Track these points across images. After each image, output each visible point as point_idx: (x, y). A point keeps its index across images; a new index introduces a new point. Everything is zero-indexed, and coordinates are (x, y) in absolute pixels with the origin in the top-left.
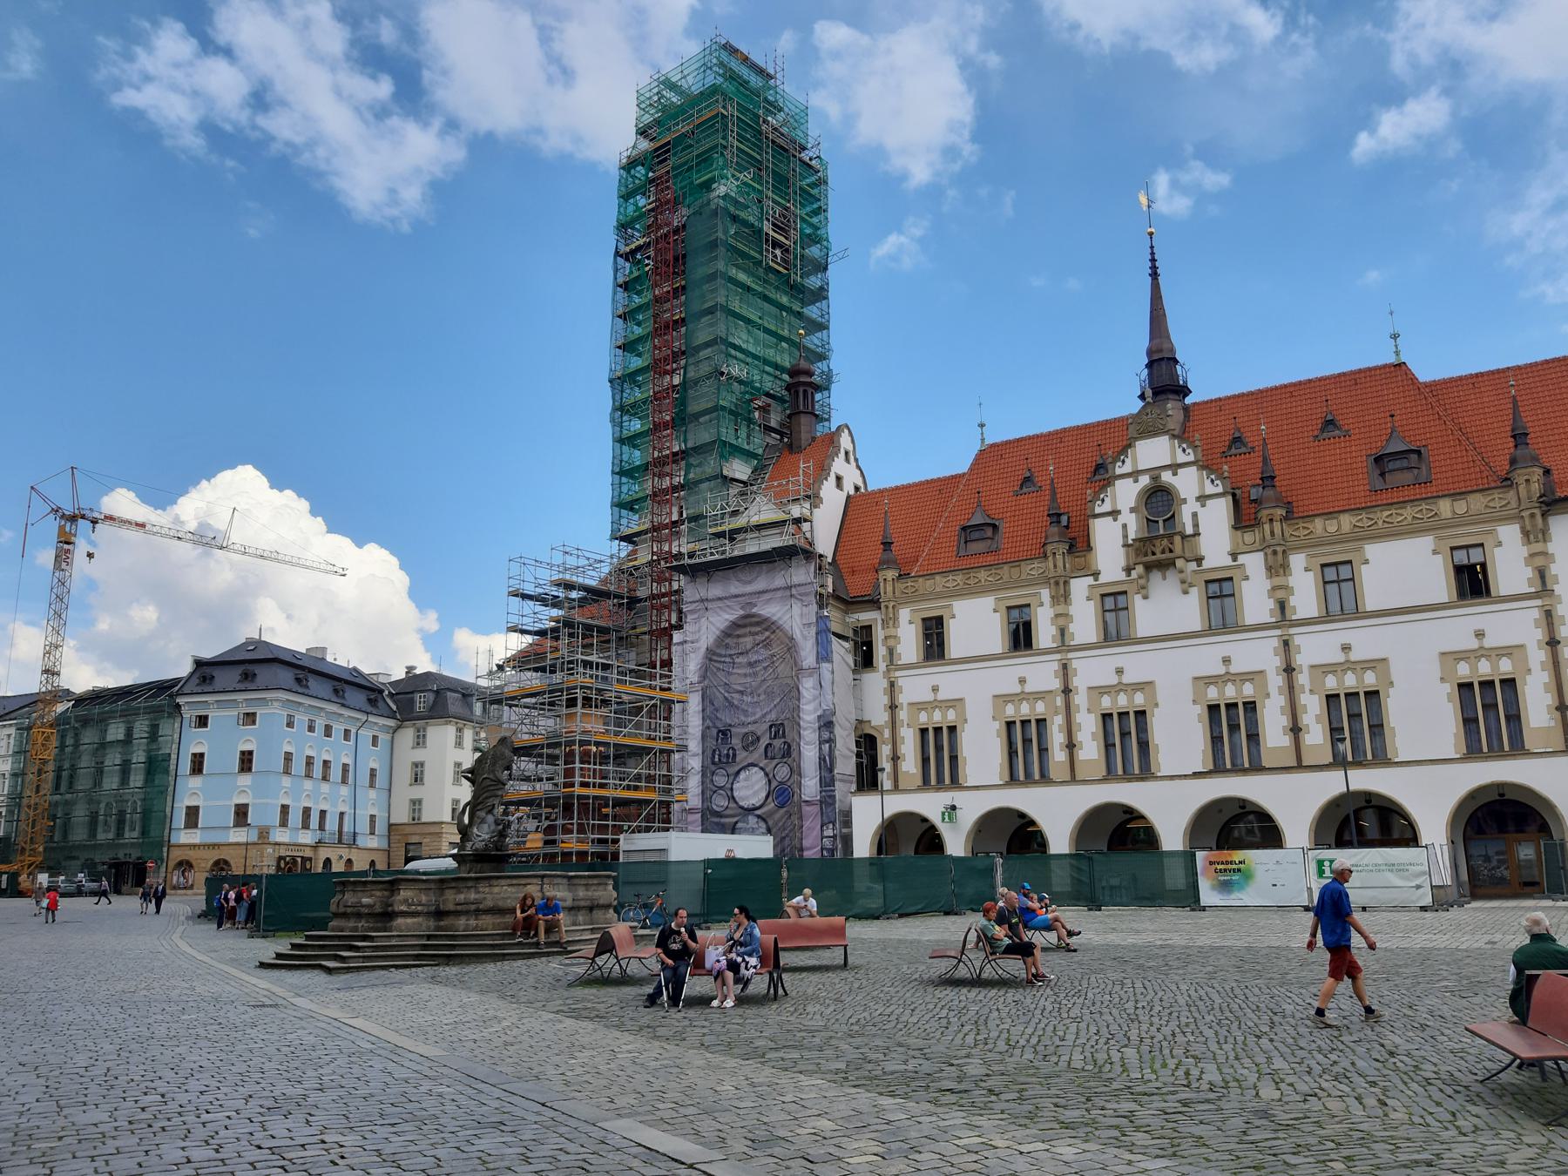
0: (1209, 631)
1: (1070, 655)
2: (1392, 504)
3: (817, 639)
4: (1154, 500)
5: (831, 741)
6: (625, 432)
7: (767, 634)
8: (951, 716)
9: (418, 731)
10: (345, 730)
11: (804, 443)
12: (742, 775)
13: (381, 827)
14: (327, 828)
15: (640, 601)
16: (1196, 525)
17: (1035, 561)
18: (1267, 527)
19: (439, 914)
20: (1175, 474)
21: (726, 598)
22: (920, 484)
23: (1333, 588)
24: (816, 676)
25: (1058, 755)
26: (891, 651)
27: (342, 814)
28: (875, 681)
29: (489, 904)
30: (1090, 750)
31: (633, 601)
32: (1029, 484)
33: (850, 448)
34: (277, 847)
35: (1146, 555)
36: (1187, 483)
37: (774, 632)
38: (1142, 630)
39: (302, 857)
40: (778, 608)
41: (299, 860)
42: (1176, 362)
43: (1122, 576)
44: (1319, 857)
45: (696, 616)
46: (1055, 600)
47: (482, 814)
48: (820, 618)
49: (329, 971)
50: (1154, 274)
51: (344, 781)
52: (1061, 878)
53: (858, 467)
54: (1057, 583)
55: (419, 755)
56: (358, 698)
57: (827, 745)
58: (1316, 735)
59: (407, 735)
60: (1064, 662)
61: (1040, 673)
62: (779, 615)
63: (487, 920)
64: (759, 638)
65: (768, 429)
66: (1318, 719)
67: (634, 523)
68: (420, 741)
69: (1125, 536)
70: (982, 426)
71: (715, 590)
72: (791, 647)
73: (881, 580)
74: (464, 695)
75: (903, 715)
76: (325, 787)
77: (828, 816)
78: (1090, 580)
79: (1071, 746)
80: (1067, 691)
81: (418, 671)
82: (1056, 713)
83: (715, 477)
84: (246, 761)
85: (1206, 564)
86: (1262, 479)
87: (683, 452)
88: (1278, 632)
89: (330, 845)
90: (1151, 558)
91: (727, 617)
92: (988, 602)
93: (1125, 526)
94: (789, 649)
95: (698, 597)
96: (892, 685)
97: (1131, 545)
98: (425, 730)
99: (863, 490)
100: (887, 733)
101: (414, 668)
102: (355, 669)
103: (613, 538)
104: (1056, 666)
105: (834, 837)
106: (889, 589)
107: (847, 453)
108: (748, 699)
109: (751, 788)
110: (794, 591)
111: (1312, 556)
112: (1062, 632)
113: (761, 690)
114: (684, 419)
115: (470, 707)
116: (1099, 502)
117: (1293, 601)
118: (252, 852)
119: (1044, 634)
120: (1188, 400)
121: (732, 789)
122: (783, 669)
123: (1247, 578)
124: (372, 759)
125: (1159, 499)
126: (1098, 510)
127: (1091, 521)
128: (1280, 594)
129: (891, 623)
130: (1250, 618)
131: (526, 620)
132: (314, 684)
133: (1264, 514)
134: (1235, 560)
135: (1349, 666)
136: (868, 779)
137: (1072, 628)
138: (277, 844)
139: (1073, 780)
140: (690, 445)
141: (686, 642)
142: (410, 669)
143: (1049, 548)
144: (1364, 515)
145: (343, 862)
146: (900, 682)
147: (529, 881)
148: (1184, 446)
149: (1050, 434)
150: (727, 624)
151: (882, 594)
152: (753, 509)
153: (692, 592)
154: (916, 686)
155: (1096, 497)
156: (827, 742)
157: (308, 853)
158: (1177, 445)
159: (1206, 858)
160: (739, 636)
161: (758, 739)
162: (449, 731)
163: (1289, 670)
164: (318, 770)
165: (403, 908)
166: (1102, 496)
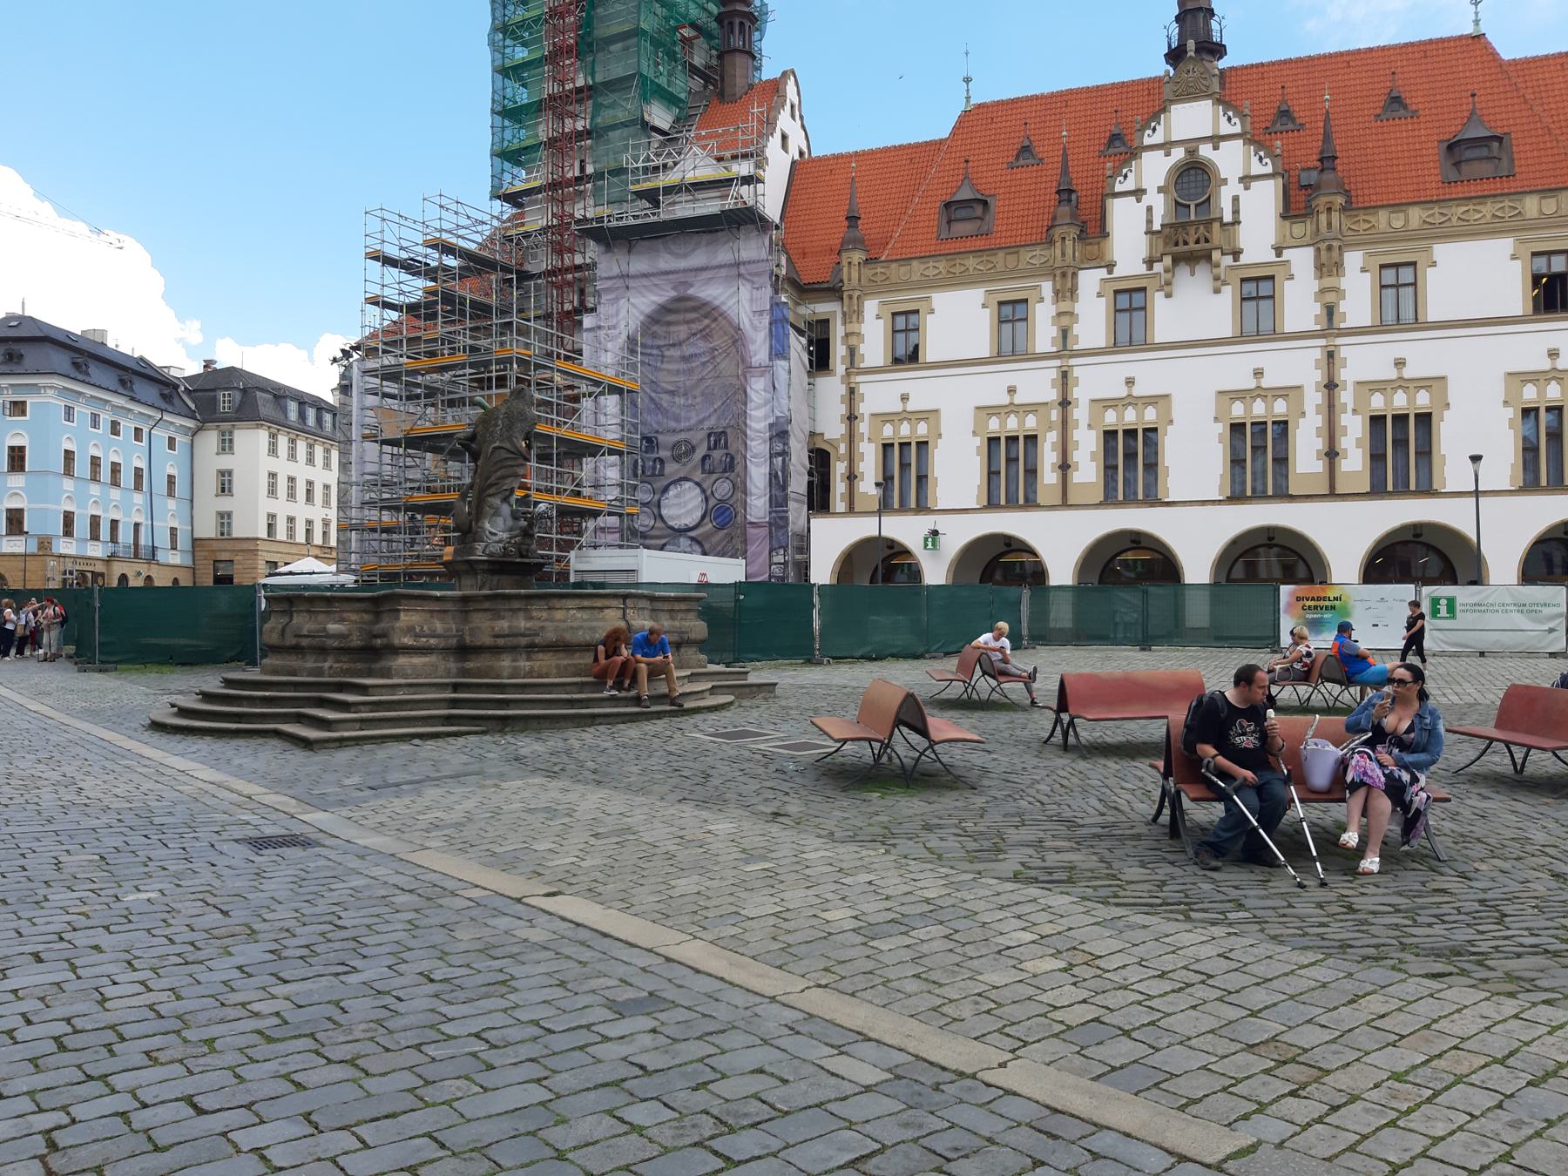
0: (1241, 338)
1: (1072, 362)
2: (1471, 198)
3: (771, 330)
4: (1186, 179)
5: (784, 454)
6: (507, 61)
7: (707, 322)
8: (922, 429)
10: (136, 429)
11: (739, 90)
12: (672, 492)
13: (183, 542)
14: (121, 539)
15: (532, 277)
16: (1236, 212)
17: (1038, 248)
18: (1323, 218)
19: (463, 651)
20: (1216, 148)
21: (653, 275)
22: (886, 150)
23: (1391, 292)
24: (768, 376)
25: (1049, 476)
26: (852, 351)
27: (137, 525)
28: (831, 387)
29: (551, 636)
30: (1087, 471)
31: (524, 276)
32: (1027, 154)
35: (1177, 244)
36: (1230, 160)
37: (715, 319)
38: (1160, 336)
40: (719, 291)
41: (89, 575)
42: (1211, 13)
43: (1142, 270)
44: (1434, 595)
45: (611, 296)
46: (1058, 295)
47: (496, 501)
48: (775, 305)
49: (307, 744)
51: (138, 486)
52: (1062, 615)
53: (803, 127)
54: (1064, 275)
55: (225, 462)
56: (150, 392)
57: (780, 459)
58: (1354, 461)
59: (210, 439)
60: (1064, 369)
61: (1037, 384)
62: (722, 299)
63: (545, 661)
64: (696, 327)
65: (694, 70)
66: (1359, 443)
67: (520, 180)
68: (226, 446)
69: (1150, 221)
70: (967, 80)
71: (639, 264)
72: (737, 338)
73: (845, 263)
74: (275, 396)
75: (863, 427)
76: (115, 494)
77: (779, 541)
78: (1103, 273)
79: (1065, 467)
80: (1065, 403)
81: (218, 366)
82: (1050, 429)
83: (632, 123)
84: (17, 459)
85: (1244, 259)
86: (1321, 160)
87: (590, 88)
88: (1322, 342)
90: (1181, 248)
91: (654, 298)
92: (976, 295)
93: (1149, 209)
94: (735, 342)
95: (616, 271)
96: (852, 391)
97: (1158, 232)
98: (231, 433)
100: (843, 449)
101: (214, 362)
102: (142, 359)
103: (495, 196)
105: (785, 563)
106: (855, 275)
107: (792, 106)
108: (681, 401)
109: (684, 506)
110: (742, 270)
111: (1370, 255)
112: (1065, 333)
113: (697, 392)
114: (590, 44)
115: (285, 411)
116: (1121, 178)
117: (1343, 306)
118: (32, 565)
119: (1044, 334)
120: (1223, 64)
121: (659, 507)
122: (727, 366)
123: (1291, 277)
124: (169, 464)
125: (1192, 178)
126: (1118, 188)
127: (1109, 201)
128: (1330, 297)
129: (855, 316)
130: (1290, 326)
131: (387, 292)
132: (95, 371)
133: (1322, 201)
134: (1279, 255)
135: (1402, 384)
136: (819, 500)
137: (1077, 329)
138: (60, 556)
139: (1065, 504)
140: (599, 78)
141: (599, 327)
142: (208, 364)
143: (1057, 232)
144: (1437, 210)
146: (862, 389)
147: (606, 602)
148: (1230, 113)
149: (1052, 95)
150: (653, 307)
151: (846, 281)
152: (689, 164)
153: (608, 265)
154: (879, 395)
155: (1117, 172)
156: (779, 454)
157: (99, 568)
158: (1221, 113)
159: (1291, 594)
160: (669, 324)
161: (693, 449)
162: (262, 436)
163: (1331, 386)
164: (105, 473)
165: (407, 641)
166: (1124, 171)
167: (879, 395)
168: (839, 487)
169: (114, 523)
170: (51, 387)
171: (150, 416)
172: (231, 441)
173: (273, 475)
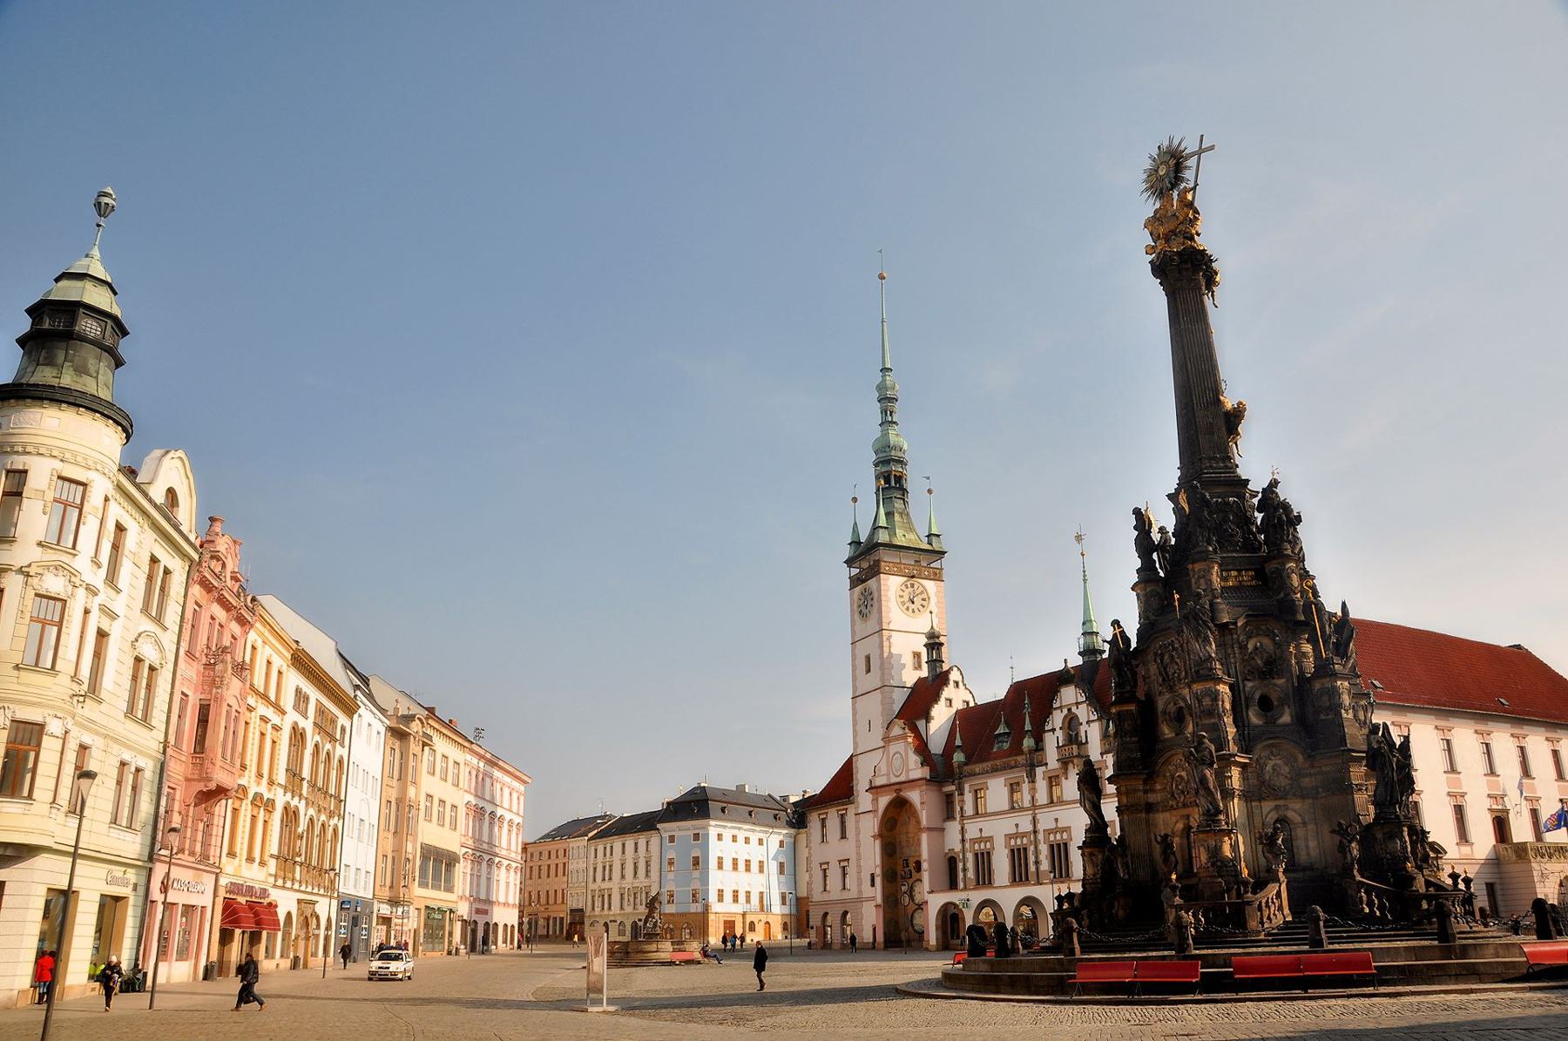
20: (1077, 708)
25: (1032, 868)
26: (962, 809)
27: (762, 893)
28: (953, 828)
33: (960, 679)
36: (1083, 712)
50: (1085, 581)
75: (967, 845)
80: (1035, 832)
99: (972, 704)
100: (961, 855)
104: (1030, 818)
107: (957, 683)
112: (1033, 798)
137: (1037, 796)
145: (762, 924)
146: (966, 827)
167: (972, 831)
168: (961, 875)
169: (748, 893)
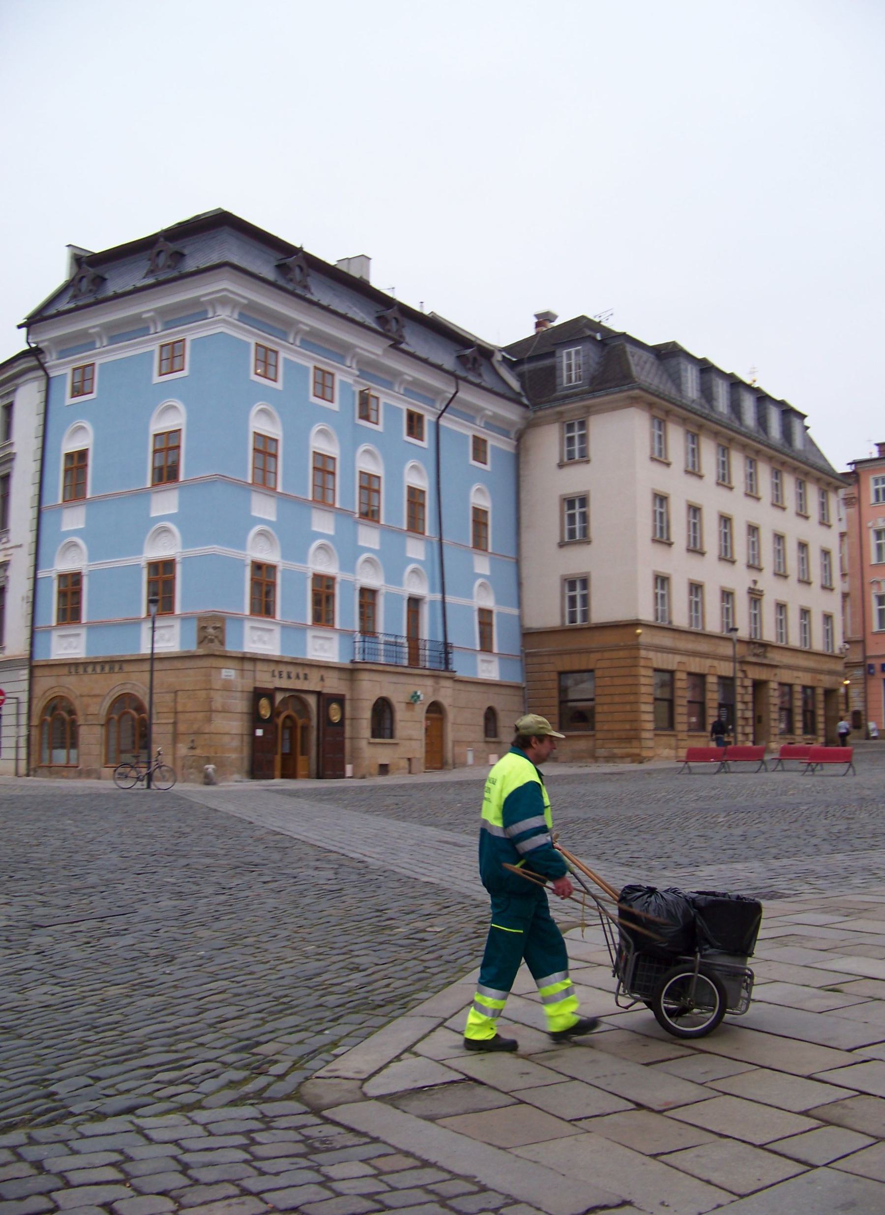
9: (570, 428)
34: (248, 666)
39: (319, 694)
41: (312, 701)
51: (415, 525)
89: (391, 670)
98: (583, 425)
115: (676, 380)
138: (254, 659)
142: (543, 319)
145: (420, 711)
157: (333, 685)
169: (368, 596)
170: (224, 302)
171: (438, 392)
172: (583, 438)
173: (661, 499)
